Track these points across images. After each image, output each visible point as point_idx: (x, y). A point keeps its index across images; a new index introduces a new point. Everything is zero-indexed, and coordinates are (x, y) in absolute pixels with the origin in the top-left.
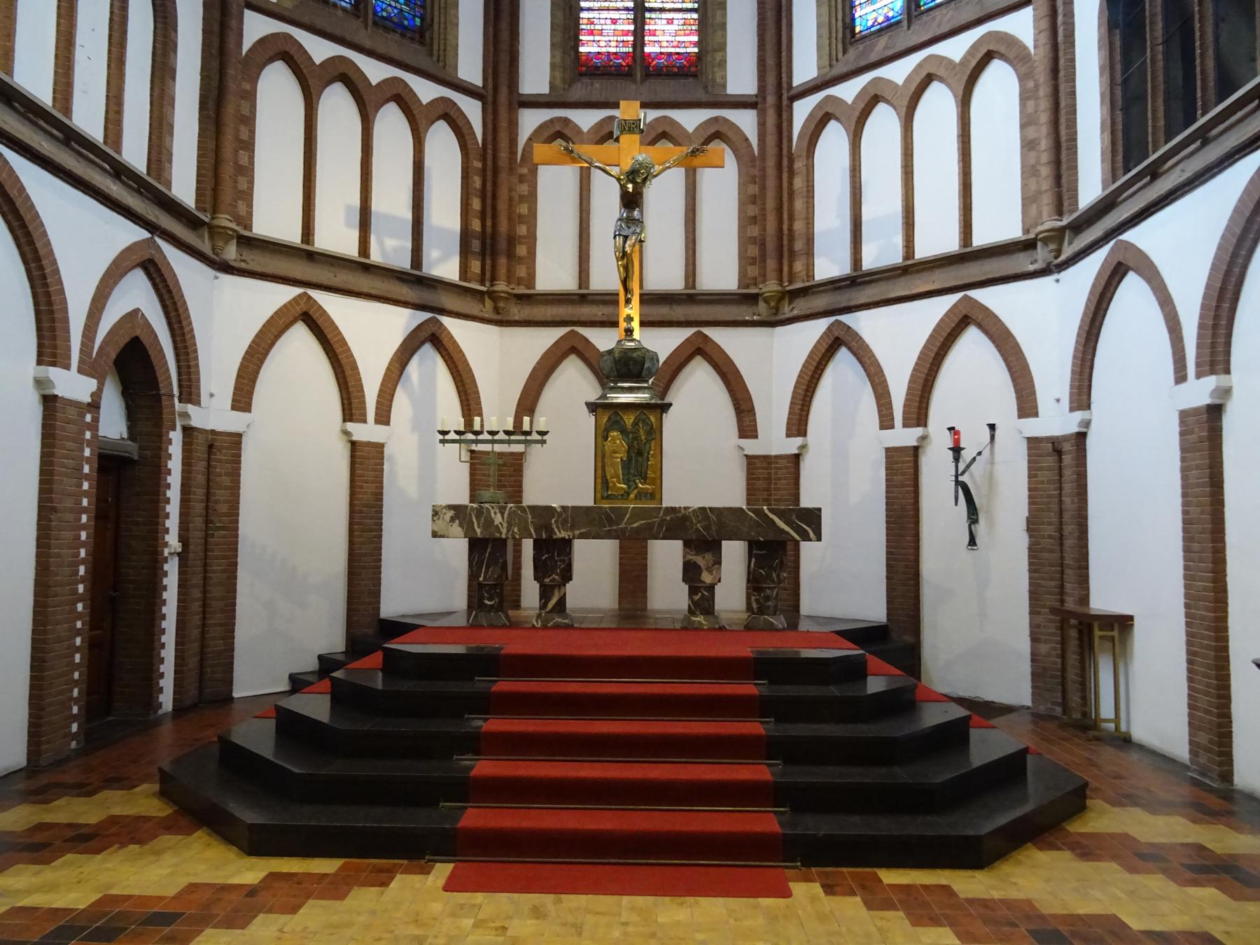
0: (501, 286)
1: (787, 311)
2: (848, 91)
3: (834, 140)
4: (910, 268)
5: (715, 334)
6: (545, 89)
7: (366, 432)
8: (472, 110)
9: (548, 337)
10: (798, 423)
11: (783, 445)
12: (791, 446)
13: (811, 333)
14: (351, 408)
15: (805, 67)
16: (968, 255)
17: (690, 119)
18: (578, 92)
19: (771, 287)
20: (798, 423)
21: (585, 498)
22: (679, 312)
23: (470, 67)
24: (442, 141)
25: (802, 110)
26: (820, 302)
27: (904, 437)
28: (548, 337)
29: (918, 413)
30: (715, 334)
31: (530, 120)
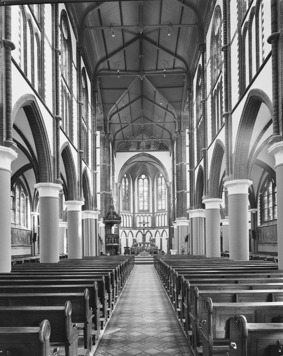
0: (135, 227)
1: (154, 228)
2: (158, 214)
3: (157, 217)
4: (162, 227)
5: (149, 230)
6: (137, 212)
7: (127, 238)
8: (132, 215)
9: (138, 231)
10: (155, 237)
11: (154, 238)
12: (155, 238)
13: (156, 230)
14: (126, 237)
15: (155, 212)
16: (164, 227)
17: (148, 215)
18: (140, 213)
19: (153, 227)
20: (155, 237)
21: (142, 242)
22: (147, 229)
23: (132, 212)
24: (130, 217)
25: (155, 214)
26: (157, 228)
27: (161, 237)
28: (138, 231)
29: (162, 236)
30: (149, 230)
31: (136, 215)
